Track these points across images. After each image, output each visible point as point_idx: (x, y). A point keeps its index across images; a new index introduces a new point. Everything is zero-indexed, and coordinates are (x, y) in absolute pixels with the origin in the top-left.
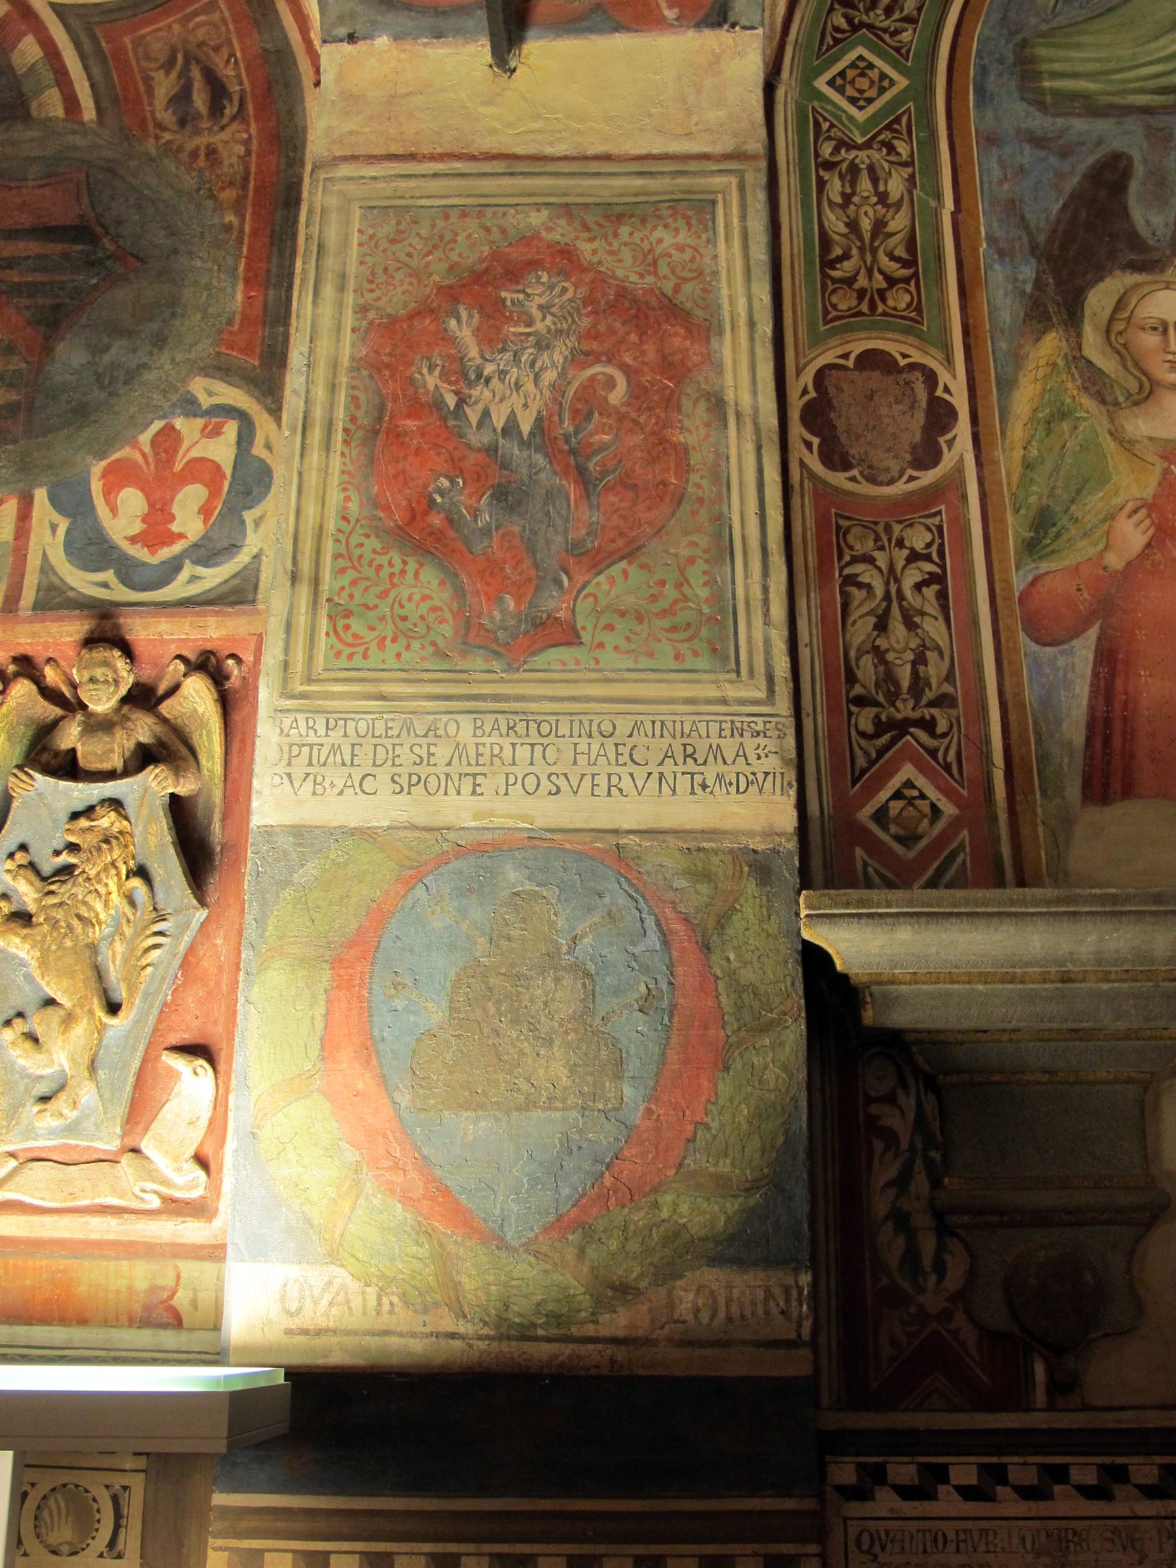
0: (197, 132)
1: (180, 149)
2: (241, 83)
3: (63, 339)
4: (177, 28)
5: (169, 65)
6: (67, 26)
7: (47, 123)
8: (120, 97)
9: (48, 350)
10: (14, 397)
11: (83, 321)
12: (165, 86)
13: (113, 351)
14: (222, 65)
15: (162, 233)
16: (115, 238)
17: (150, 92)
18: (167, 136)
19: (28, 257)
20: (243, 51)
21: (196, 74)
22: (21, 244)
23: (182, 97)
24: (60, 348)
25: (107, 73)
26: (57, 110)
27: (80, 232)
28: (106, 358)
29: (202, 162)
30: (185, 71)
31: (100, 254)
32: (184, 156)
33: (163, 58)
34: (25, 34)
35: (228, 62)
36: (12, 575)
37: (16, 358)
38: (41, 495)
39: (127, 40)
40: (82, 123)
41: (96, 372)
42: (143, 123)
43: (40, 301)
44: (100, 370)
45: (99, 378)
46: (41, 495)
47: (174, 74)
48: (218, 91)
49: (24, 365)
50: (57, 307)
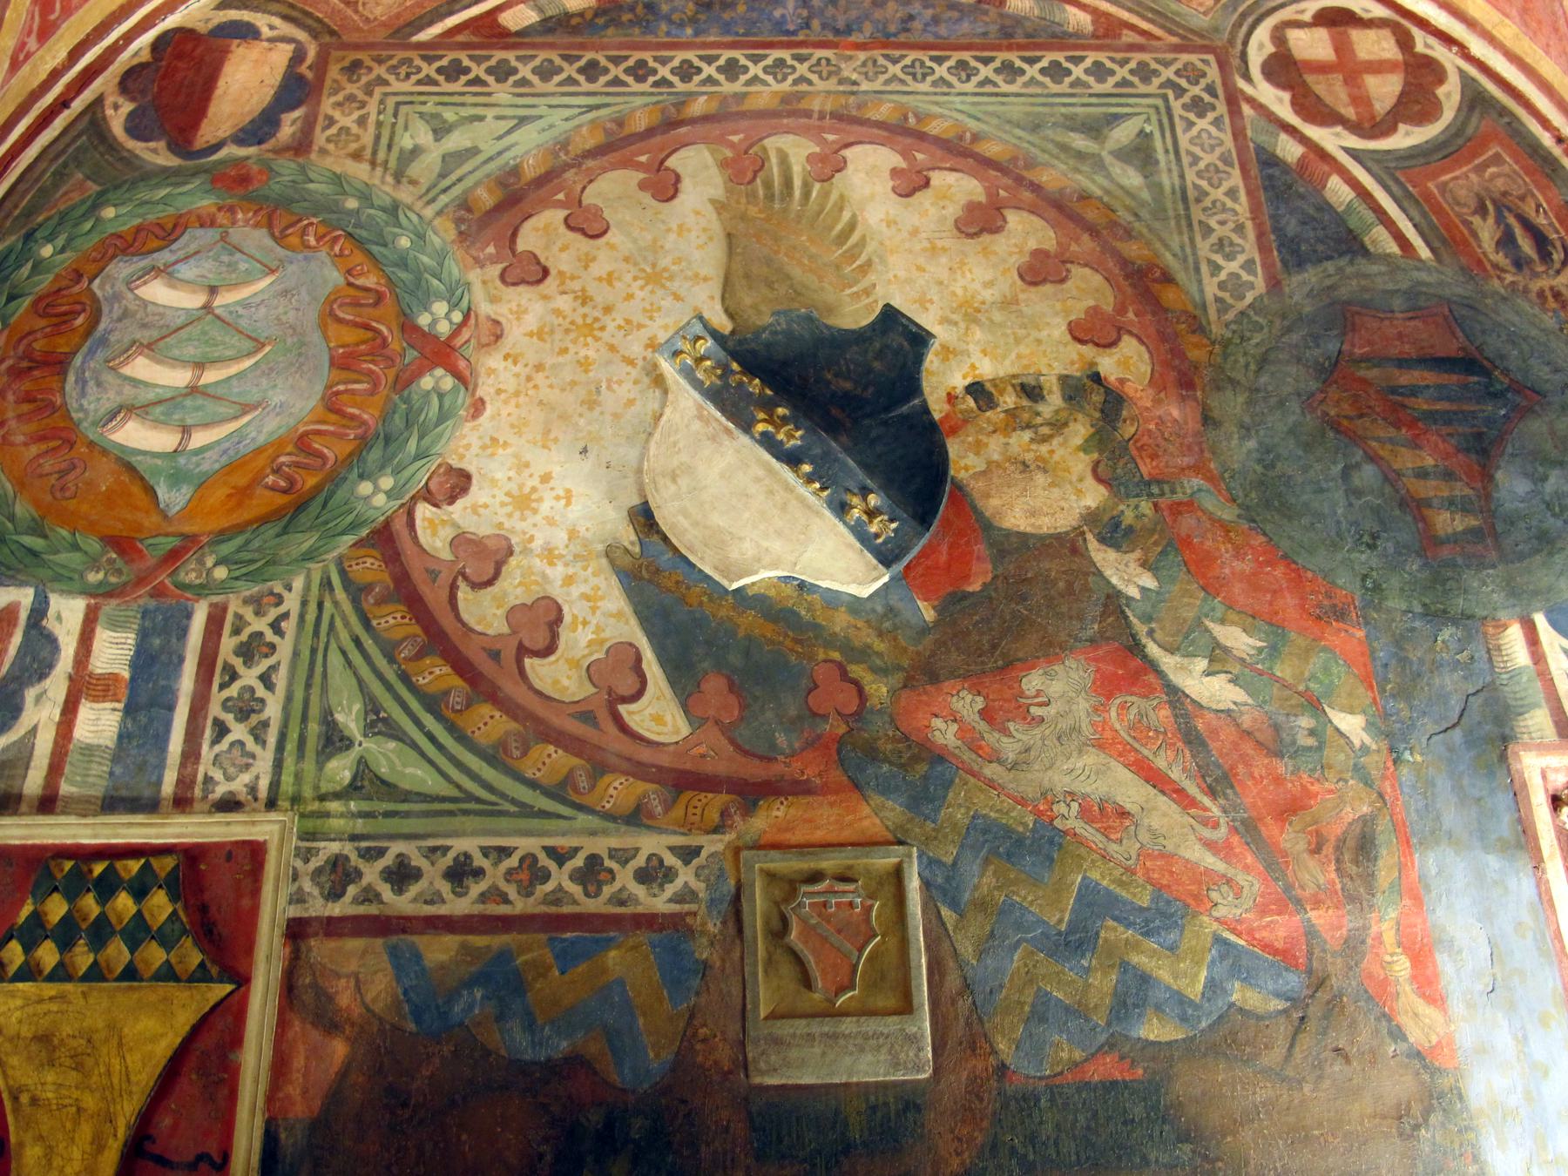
0: (1535, 275)
1: (1526, 291)
2: (1557, 232)
3: (1498, 467)
4: (1473, 177)
5: (1482, 210)
6: (1368, 170)
7: (1386, 258)
8: (1449, 238)
9: (1487, 476)
10: (1473, 522)
11: (1509, 449)
12: (1487, 232)
13: (1552, 480)
14: (1533, 214)
15: (1547, 369)
16: (1506, 372)
17: (1475, 234)
18: (1509, 278)
19: (1427, 386)
20: (1548, 203)
21: (1512, 220)
22: (1416, 373)
23: (1506, 241)
24: (1499, 475)
25: (1424, 215)
26: (1393, 248)
27: (1468, 364)
28: (1549, 487)
29: (1552, 303)
30: (1500, 219)
31: (1498, 387)
32: (1533, 296)
33: (1473, 204)
34: (1329, 175)
35: (1537, 211)
36: (1548, 701)
37: (1459, 484)
38: (1540, 619)
39: (1431, 185)
40: (1420, 260)
41: (1544, 502)
42: (1479, 263)
43: (1460, 430)
44: (1547, 498)
45: (1548, 505)
46: (1540, 619)
47: (1491, 220)
48: (1541, 240)
49: (1467, 491)
50: (1479, 436)
